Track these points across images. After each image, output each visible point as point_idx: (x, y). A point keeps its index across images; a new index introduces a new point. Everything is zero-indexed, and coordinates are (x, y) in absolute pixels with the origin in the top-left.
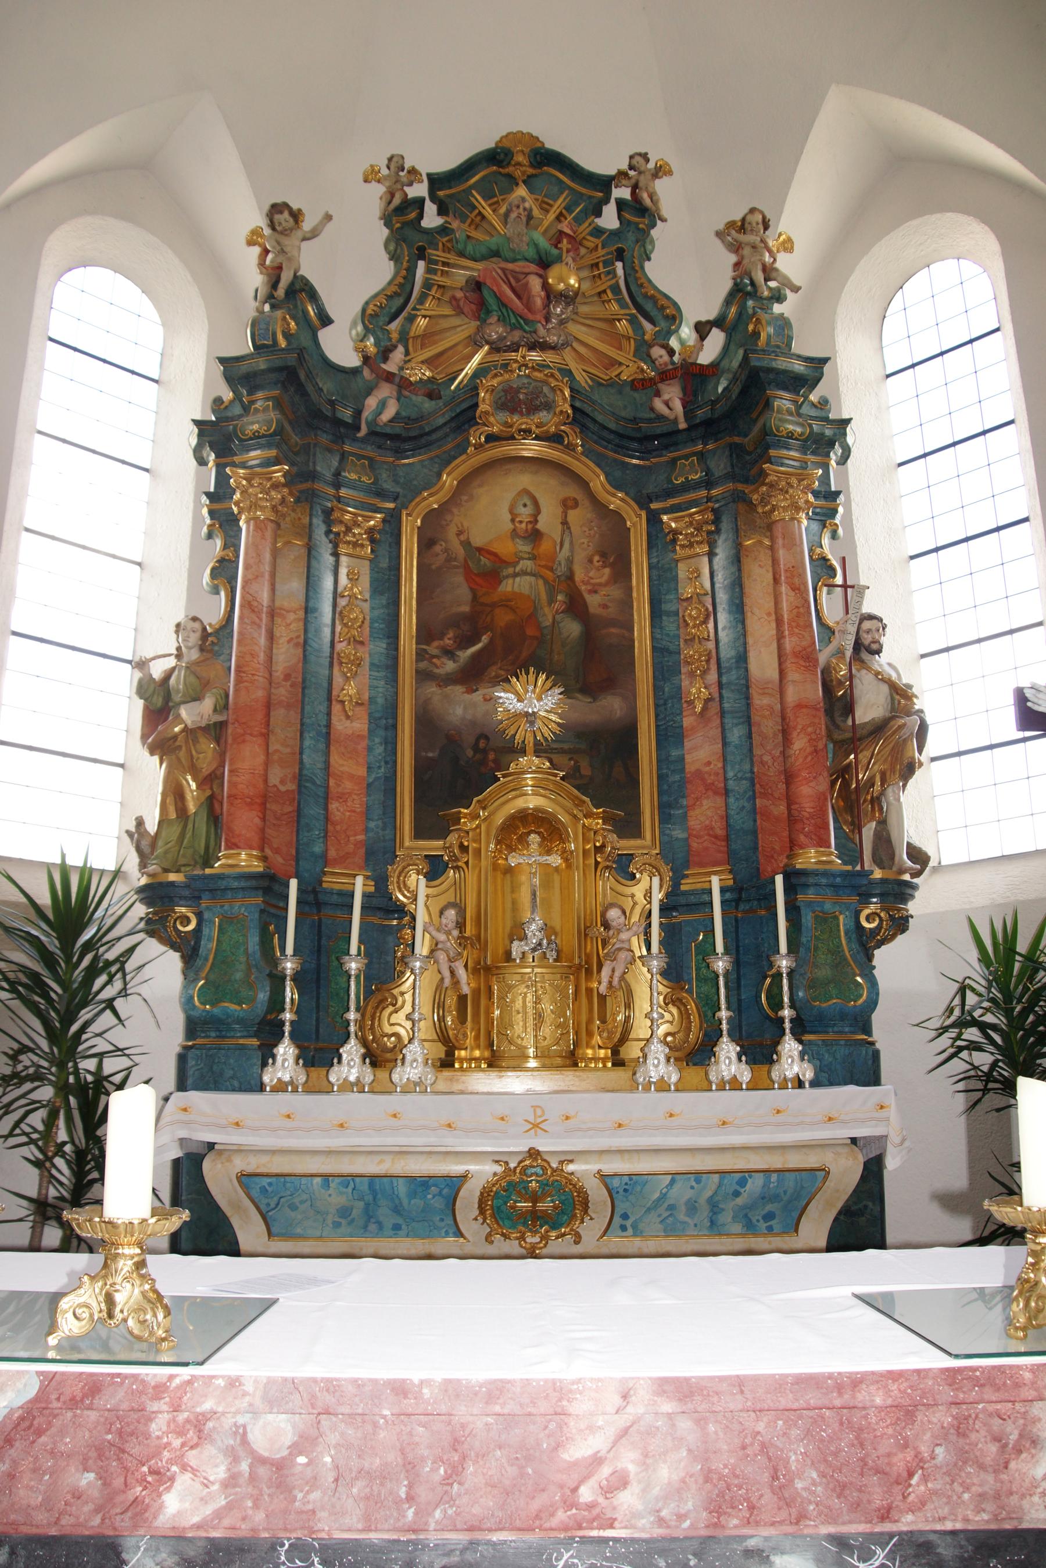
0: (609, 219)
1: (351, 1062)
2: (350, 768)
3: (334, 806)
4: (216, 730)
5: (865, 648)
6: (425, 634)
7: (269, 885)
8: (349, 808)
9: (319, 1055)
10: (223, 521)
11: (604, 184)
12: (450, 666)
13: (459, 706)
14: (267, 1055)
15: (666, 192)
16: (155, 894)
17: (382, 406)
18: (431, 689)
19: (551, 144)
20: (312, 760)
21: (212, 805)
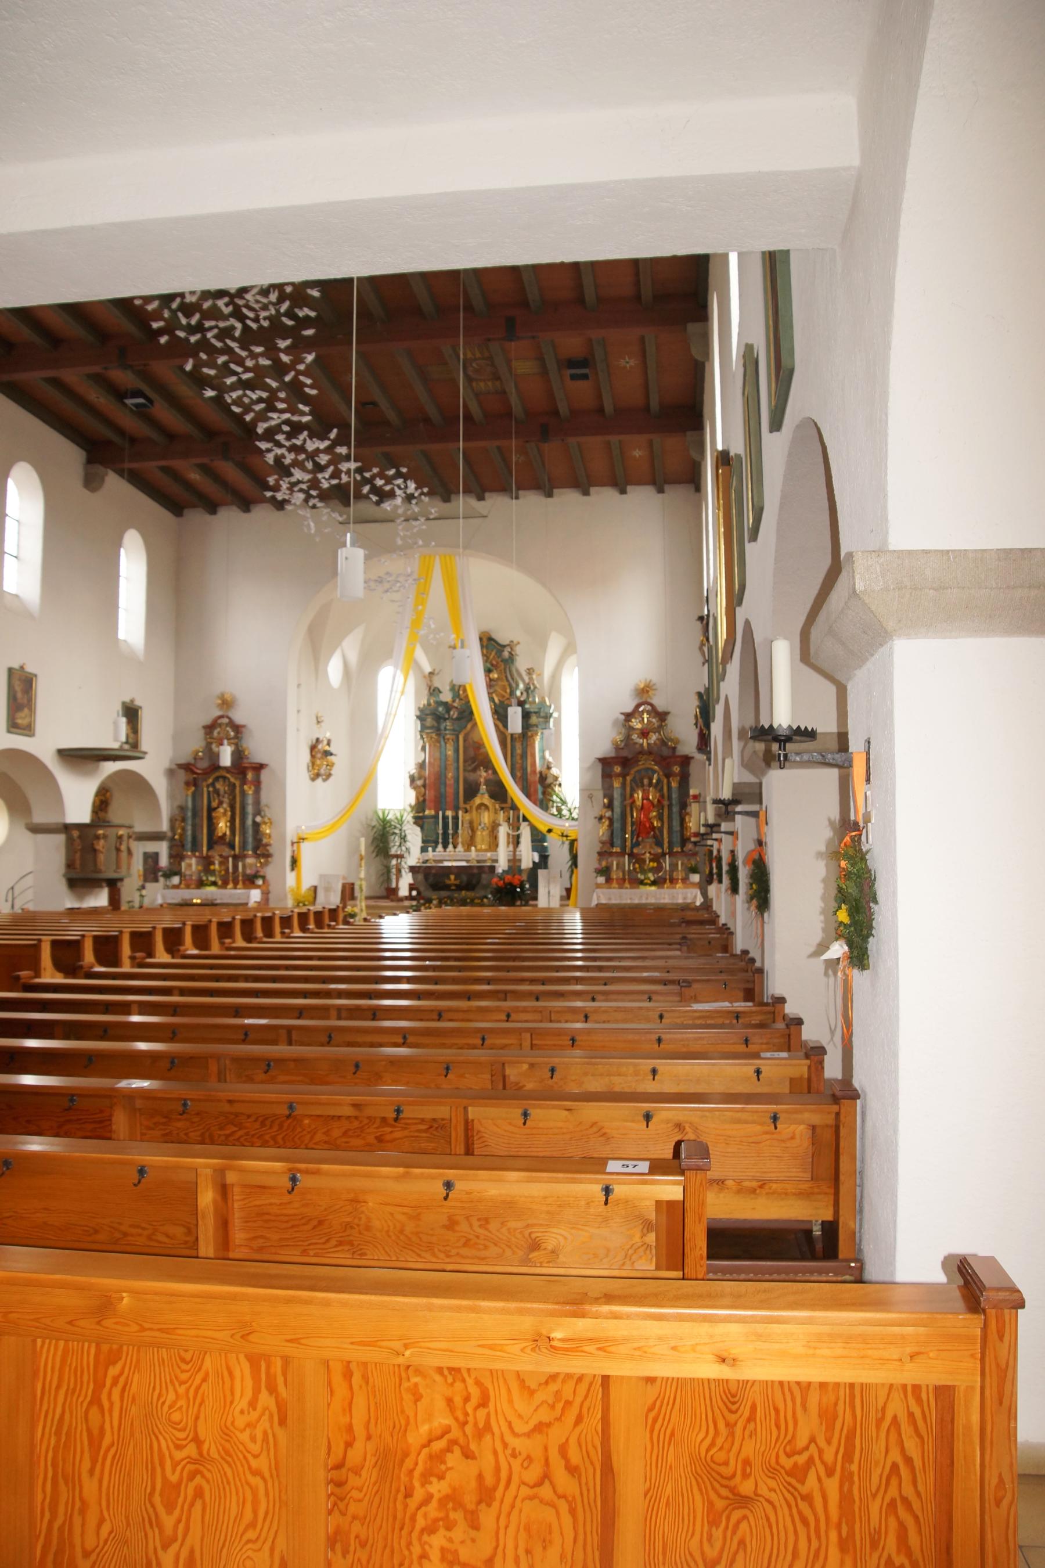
0: (506, 654)
1: (451, 846)
2: (450, 791)
3: (448, 799)
4: (424, 786)
5: (549, 768)
6: (465, 761)
7: (436, 817)
8: (450, 799)
9: (445, 847)
10: (422, 737)
11: (505, 646)
12: (470, 768)
13: (472, 776)
14: (436, 847)
15: (518, 650)
16: (415, 818)
17: (454, 714)
18: (467, 774)
19: (494, 636)
20: (443, 790)
21: (424, 801)
